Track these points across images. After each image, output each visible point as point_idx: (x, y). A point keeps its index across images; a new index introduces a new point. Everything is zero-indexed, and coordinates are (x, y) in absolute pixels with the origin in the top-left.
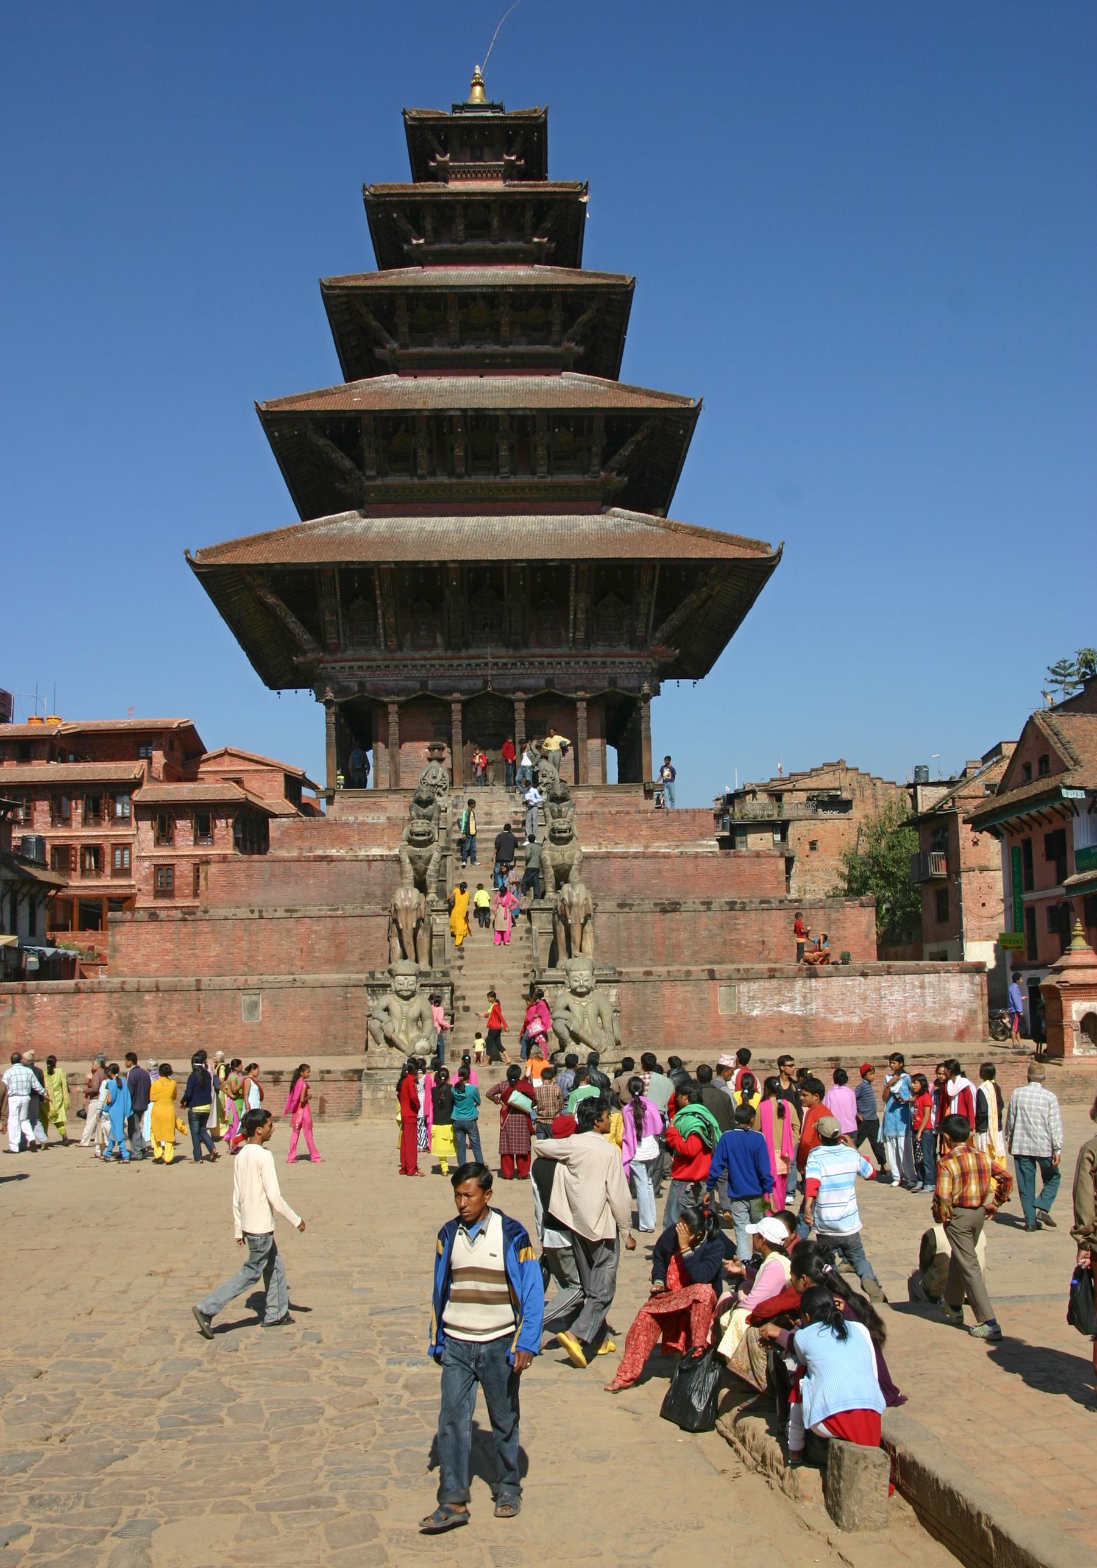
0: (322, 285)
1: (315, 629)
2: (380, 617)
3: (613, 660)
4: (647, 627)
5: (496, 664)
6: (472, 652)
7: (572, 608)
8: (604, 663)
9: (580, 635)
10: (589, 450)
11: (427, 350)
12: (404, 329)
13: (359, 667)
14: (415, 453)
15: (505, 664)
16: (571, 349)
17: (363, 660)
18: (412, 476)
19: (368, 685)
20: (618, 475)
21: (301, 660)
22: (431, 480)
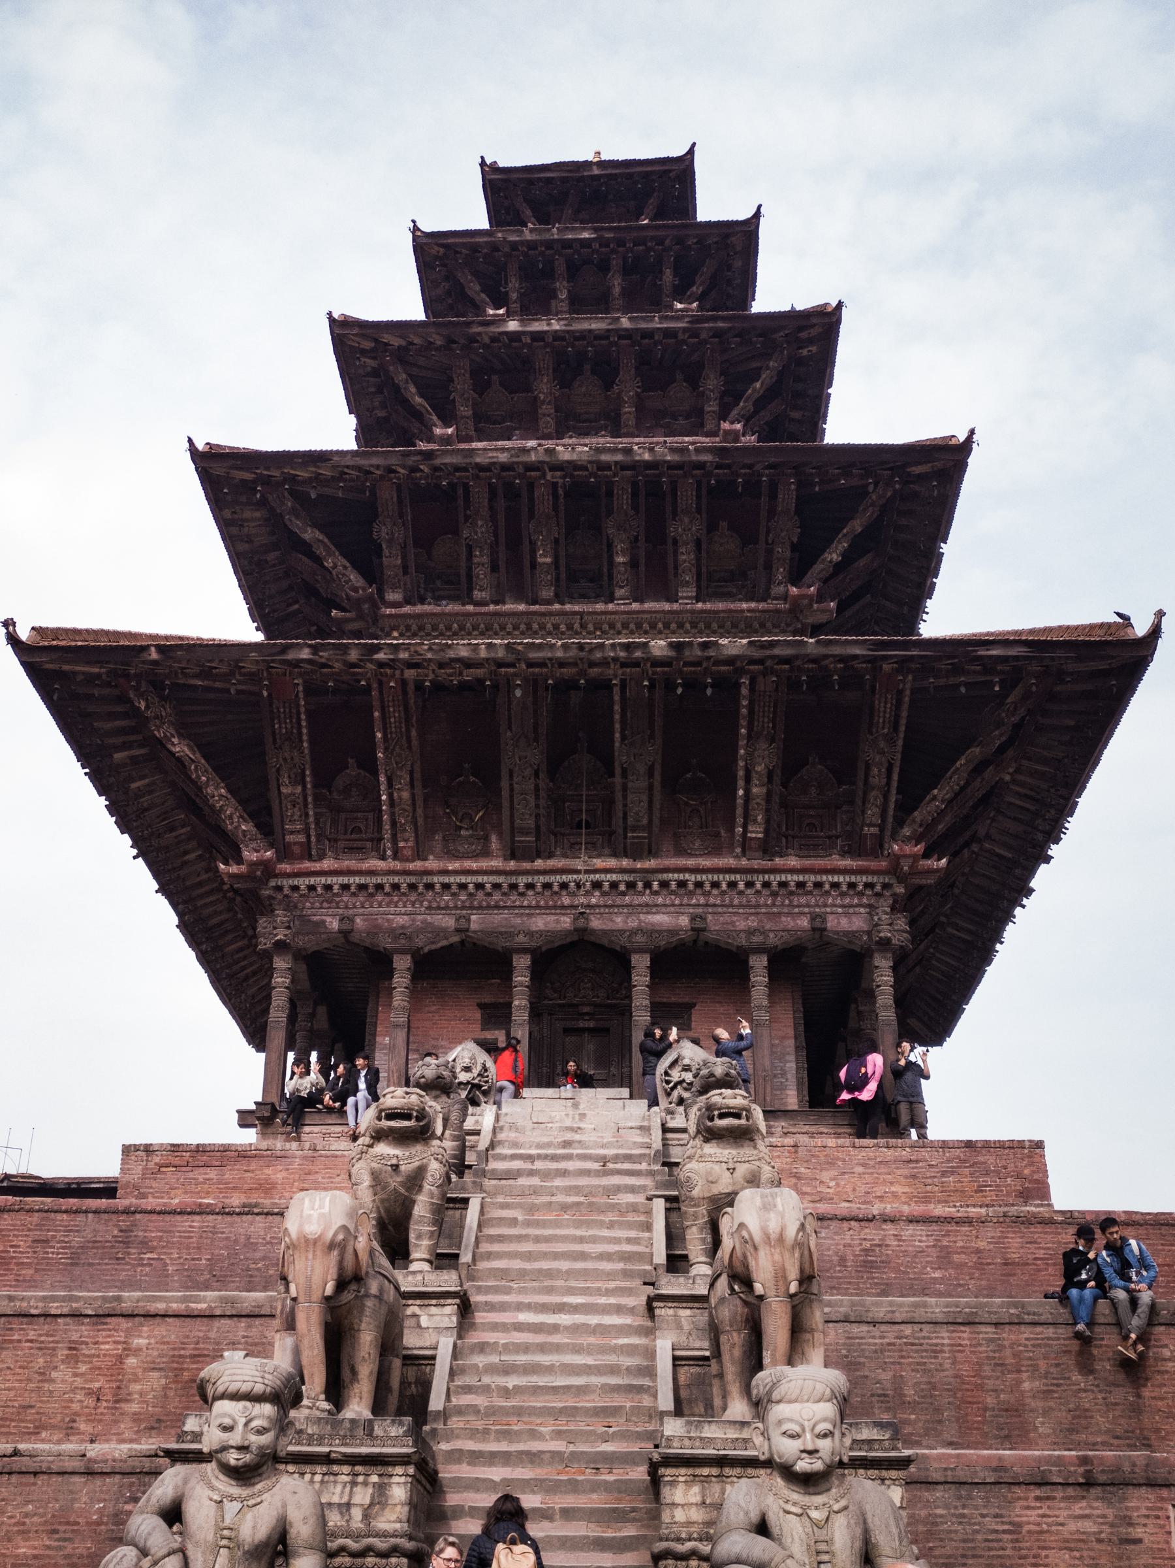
2: (382, 788)
3: (819, 878)
4: (884, 815)
5: (597, 885)
7: (741, 773)
8: (801, 885)
9: (756, 832)
10: (768, 567)
12: (464, 410)
13: (345, 887)
15: (614, 885)
16: (736, 432)
17: (350, 872)
18: (463, 605)
19: (358, 920)
21: (234, 869)
22: (492, 607)
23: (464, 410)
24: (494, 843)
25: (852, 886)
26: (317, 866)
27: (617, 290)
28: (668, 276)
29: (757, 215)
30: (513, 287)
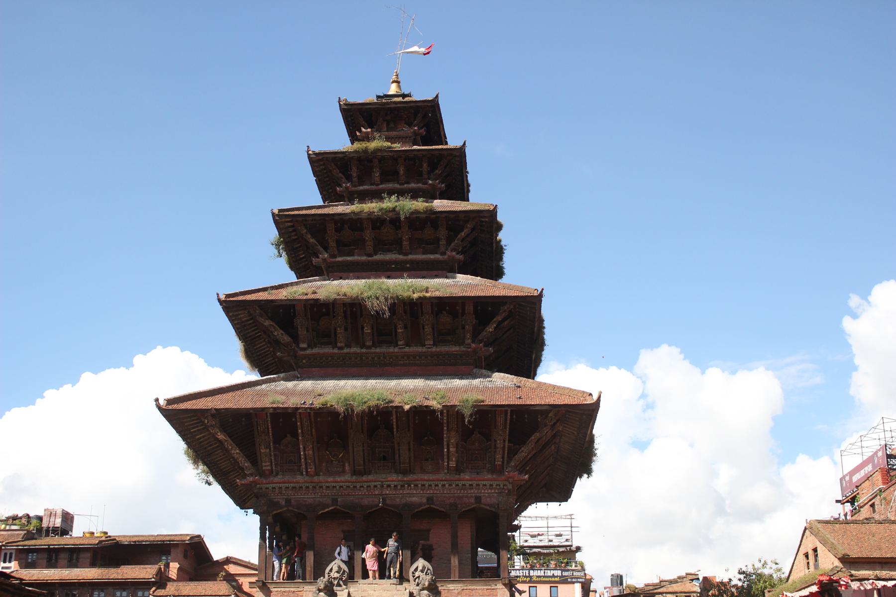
0: (273, 214)
1: (254, 459)
4: (503, 458)
5: (389, 486)
6: (371, 477)
9: (453, 464)
10: (463, 328)
11: (349, 258)
12: (332, 244)
14: (335, 330)
15: (396, 486)
16: (453, 257)
20: (485, 346)
22: (346, 350)
23: (332, 244)
24: (347, 468)
25: (491, 485)
26: (276, 479)
27: (402, 172)
28: (425, 165)
29: (465, 144)
30: (354, 173)
